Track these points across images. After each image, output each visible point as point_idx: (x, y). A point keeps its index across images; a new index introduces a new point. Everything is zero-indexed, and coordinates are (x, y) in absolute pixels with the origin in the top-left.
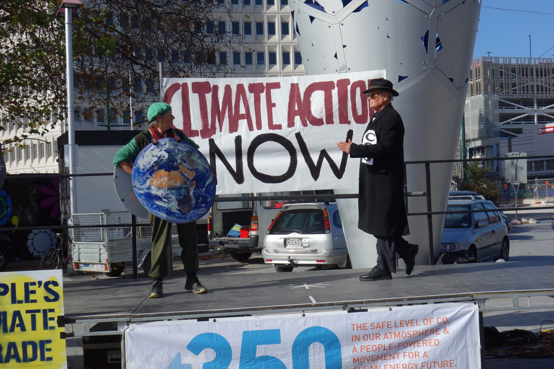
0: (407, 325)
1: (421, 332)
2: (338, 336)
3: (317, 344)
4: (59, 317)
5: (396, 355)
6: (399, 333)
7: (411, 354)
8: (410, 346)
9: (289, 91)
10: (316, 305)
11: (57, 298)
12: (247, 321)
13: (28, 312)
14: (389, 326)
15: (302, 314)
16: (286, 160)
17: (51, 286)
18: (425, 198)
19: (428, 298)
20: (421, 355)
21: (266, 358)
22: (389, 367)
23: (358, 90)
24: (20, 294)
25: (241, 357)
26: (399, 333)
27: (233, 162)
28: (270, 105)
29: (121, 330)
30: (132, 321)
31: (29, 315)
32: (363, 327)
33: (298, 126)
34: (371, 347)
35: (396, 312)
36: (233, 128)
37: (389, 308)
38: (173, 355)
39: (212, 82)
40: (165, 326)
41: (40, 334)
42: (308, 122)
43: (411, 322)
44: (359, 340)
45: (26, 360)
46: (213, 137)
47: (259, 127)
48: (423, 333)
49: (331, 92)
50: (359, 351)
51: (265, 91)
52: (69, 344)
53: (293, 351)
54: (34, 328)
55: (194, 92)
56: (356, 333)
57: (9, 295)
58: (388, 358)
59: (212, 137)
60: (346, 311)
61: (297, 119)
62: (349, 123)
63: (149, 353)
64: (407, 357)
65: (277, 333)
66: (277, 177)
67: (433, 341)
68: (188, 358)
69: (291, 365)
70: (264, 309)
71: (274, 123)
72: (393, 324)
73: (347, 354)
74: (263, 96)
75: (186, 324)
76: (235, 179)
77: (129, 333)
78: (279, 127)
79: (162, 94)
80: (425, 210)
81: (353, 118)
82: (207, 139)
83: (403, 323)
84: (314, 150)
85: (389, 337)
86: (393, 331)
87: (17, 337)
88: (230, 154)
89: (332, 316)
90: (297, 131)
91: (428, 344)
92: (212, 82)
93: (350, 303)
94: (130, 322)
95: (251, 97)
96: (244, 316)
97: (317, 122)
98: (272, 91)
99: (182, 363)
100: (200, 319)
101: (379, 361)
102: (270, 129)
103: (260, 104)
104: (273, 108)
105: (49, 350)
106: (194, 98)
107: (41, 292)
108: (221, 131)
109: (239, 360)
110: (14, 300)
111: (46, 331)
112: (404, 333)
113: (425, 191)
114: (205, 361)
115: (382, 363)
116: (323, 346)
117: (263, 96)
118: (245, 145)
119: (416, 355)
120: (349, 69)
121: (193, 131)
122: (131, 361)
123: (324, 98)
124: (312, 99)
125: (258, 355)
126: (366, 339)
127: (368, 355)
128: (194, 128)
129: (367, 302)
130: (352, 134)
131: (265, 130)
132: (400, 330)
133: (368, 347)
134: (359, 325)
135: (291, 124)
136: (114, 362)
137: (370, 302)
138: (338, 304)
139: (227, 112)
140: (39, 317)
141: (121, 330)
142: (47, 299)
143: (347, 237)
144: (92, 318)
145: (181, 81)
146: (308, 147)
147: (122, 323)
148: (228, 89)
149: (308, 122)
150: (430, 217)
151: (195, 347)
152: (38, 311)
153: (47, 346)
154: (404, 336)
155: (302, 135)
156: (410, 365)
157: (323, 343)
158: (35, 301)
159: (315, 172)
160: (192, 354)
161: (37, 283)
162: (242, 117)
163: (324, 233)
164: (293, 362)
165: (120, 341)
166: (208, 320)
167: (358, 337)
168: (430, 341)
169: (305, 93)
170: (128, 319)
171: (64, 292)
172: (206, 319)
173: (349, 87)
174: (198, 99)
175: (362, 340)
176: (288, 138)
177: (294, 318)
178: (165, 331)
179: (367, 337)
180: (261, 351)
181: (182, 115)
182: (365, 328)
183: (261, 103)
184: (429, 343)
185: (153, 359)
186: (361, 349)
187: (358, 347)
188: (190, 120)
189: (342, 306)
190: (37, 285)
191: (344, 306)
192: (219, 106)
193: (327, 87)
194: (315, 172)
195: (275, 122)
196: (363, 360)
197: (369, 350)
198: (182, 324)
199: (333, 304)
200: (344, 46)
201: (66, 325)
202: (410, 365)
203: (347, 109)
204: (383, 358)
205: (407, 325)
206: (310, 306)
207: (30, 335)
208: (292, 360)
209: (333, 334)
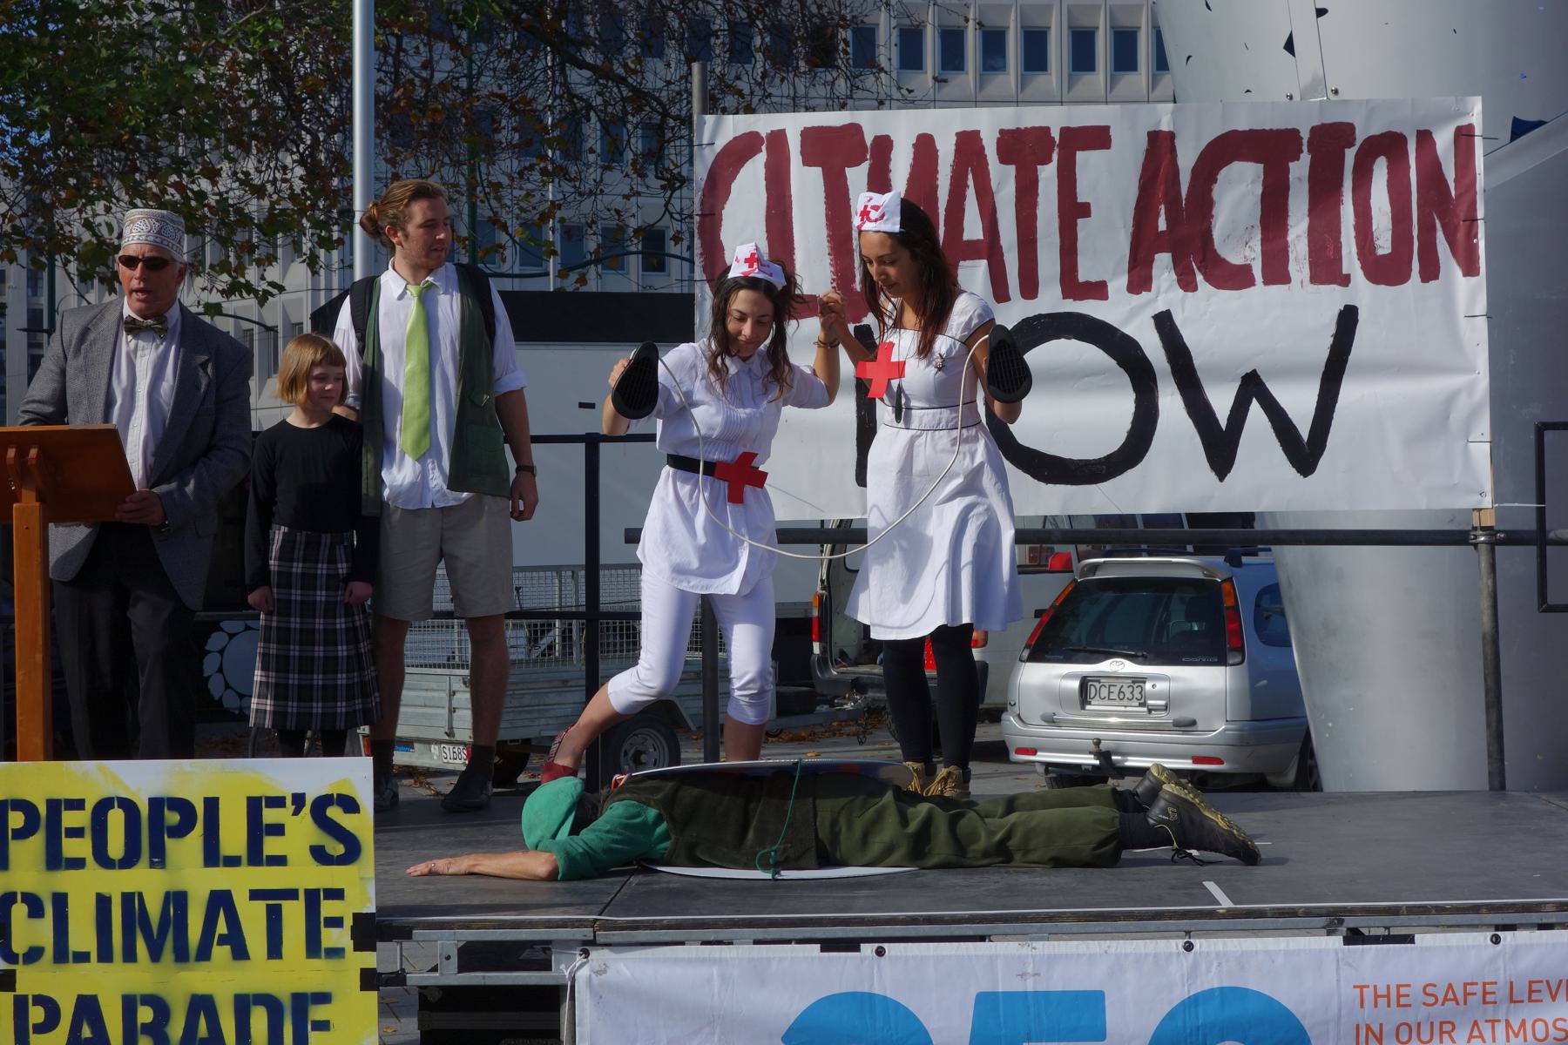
0: (1554, 998)
2: (1306, 1024)
4: (356, 916)
6: (1523, 1023)
10: (1232, 914)
12: (992, 959)
13: (255, 895)
14: (1489, 998)
15: (1181, 942)
17: (334, 813)
24: (233, 838)
26: (1523, 1023)
28: (1073, 210)
29: (563, 968)
30: (600, 940)
31: (261, 906)
32: (1397, 996)
33: (1163, 288)
35: (1516, 950)
37: (1489, 934)
39: (872, 123)
40: (713, 961)
41: (293, 973)
42: (1200, 278)
47: (1030, 289)
52: (387, 1010)
54: (275, 950)
55: (807, 162)
56: (1369, 1015)
57: (196, 836)
61: (1163, 262)
62: (1345, 281)
65: (1093, 1001)
66: (1086, 463)
70: (1050, 918)
71: (1082, 277)
72: (1502, 992)
75: (781, 959)
77: (590, 981)
79: (701, 172)
81: (1358, 264)
84: (1221, 376)
85: (1488, 1035)
89: (1288, 953)
90: (1160, 307)
92: (872, 123)
94: (593, 943)
95: (1003, 179)
96: (982, 938)
97: (1237, 278)
100: (829, 945)
102: (1065, 296)
103: (1034, 205)
104: (1080, 221)
105: (323, 1026)
106: (806, 184)
107: (300, 833)
110: (212, 856)
111: (315, 962)
112: (1540, 1026)
120: (1336, 92)
123: (1259, 189)
126: (1404, 1038)
129: (1412, 911)
131: (1050, 300)
132: (1528, 1012)
134: (1382, 991)
135: (1140, 281)
137: (1424, 910)
138: (1308, 913)
140: (294, 914)
141: (563, 968)
142: (319, 855)
143: (1308, 680)
144: (467, 925)
145: (764, 123)
146: (1198, 361)
147: (567, 945)
148: (925, 147)
149: (1200, 278)
152: (291, 894)
153: (317, 1013)
154: (1541, 1033)
155: (1178, 320)
158: (280, 861)
159: (1221, 448)
161: (289, 801)
162: (972, 251)
163: (1222, 662)
165: (556, 1008)
166: (858, 949)
167: (1377, 1032)
169: (1195, 171)
170: (587, 933)
172: (852, 945)
173: (1350, 155)
176: (1128, 330)
177: (1156, 956)
182: (1403, 1001)
183: (1040, 200)
189: (1323, 921)
190: (290, 807)
191: (1332, 921)
193: (1269, 148)
194: (1221, 448)
195: (1085, 274)
198: (769, 960)
199: (1293, 913)
200: (1321, 12)
201: (379, 944)
203: (1339, 232)
205: (1554, 998)
206: (1211, 915)
207: (260, 974)
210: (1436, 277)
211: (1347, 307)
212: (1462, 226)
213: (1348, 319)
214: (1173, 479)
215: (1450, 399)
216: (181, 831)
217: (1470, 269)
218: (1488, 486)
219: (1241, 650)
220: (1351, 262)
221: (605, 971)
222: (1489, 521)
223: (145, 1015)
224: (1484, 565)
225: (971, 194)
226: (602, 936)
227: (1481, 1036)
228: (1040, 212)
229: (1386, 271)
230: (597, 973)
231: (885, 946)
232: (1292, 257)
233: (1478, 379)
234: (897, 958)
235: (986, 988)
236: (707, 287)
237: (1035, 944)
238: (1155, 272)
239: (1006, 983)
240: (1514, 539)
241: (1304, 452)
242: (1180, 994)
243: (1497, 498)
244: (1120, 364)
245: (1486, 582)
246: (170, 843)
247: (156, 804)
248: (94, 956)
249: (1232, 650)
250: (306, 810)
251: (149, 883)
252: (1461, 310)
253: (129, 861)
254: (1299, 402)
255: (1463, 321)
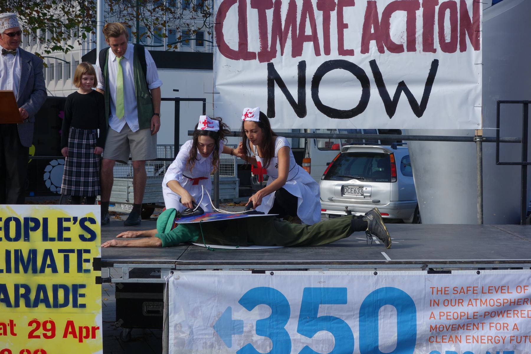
0: (497, 292)
1: (513, 301)
2: (414, 299)
3: (389, 307)
4: (94, 259)
5: (480, 325)
6: (486, 300)
7: (498, 326)
8: (499, 316)
9: (365, 9)
10: (390, 263)
11: (93, 237)
13: (60, 251)
15: (373, 272)
16: (357, 92)
17: (87, 224)
18: (520, 145)
19: (525, 262)
20: (511, 327)
21: (328, 319)
22: (471, 338)
23: (448, 12)
24: (53, 231)
25: (301, 316)
26: (486, 300)
27: (294, 92)
28: (342, 26)
30: (177, 268)
32: (444, 291)
33: (373, 52)
34: (452, 314)
35: (485, 276)
36: (297, 51)
38: (223, 309)
40: (215, 276)
41: (73, 277)
42: (385, 49)
43: (501, 289)
44: (438, 305)
45: (56, 305)
46: (273, 61)
47: (327, 52)
48: (514, 302)
49: (415, 13)
50: (437, 317)
51: (336, 8)
52: (105, 292)
53: (360, 313)
54: (67, 270)
56: (435, 297)
58: (471, 328)
59: (271, 61)
60: (425, 272)
61: (373, 44)
62: (434, 51)
63: (195, 305)
64: (493, 329)
65: (343, 291)
67: (526, 312)
68: (240, 314)
69: (358, 328)
70: (329, 263)
71: (345, 48)
72: (479, 289)
73: (423, 321)
74: (334, 15)
76: (296, 111)
77: (173, 282)
78: (351, 53)
80: (520, 160)
81: (439, 45)
82: (265, 64)
83: (491, 289)
84: (391, 82)
85: (474, 304)
86: (479, 298)
87: (48, 279)
88: (291, 83)
90: (372, 59)
91: (519, 315)
93: (431, 263)
94: (175, 269)
96: (306, 270)
97: (396, 49)
98: (345, 8)
99: (233, 319)
100: (254, 272)
101: (461, 331)
102: (340, 54)
103: (329, 24)
105: (83, 295)
106: (252, 14)
107: (76, 230)
108: (282, 54)
109: (298, 319)
110: (45, 237)
111: (80, 274)
112: (492, 302)
113: (520, 136)
114: (258, 318)
115: (463, 333)
116: (395, 309)
117: (334, 15)
118: (310, 72)
119: (505, 326)
121: (250, 52)
122: (175, 313)
123: (406, 19)
124: (391, 20)
125: (319, 315)
126: (446, 304)
127: (448, 323)
128: (250, 49)
129: (451, 263)
130: (438, 65)
131: (335, 55)
132: (488, 297)
133: (449, 314)
134: (439, 289)
135: (365, 49)
136: (150, 315)
137: (455, 263)
138: (416, 263)
139: (290, 32)
140: (73, 258)
142: (82, 238)
143: (418, 187)
144: (132, 263)
146: (384, 78)
147: (166, 269)
149: (385, 49)
150: (524, 166)
151: (249, 301)
152: (72, 251)
153: (81, 291)
154: (492, 304)
155: (378, 63)
156: (497, 338)
157: (396, 306)
158: (69, 240)
159: (391, 107)
160: (244, 309)
161: (72, 219)
163: (389, 181)
164: (360, 326)
165: (162, 291)
166: (264, 273)
167: (437, 302)
168: (523, 312)
169: (384, 13)
170: (173, 266)
171: (102, 231)
172: (263, 272)
173: (437, 8)
174: (258, 16)
175: (441, 305)
176: (361, 66)
177: (365, 276)
178: (214, 282)
179: (447, 302)
180: (323, 310)
181: (238, 34)
182: (446, 292)
183: (331, 22)
184: (521, 314)
185: (200, 313)
186: (440, 316)
187: (436, 313)
188: (247, 40)
189: (421, 266)
190: (72, 222)
191: (424, 265)
192: (281, 25)
194: (391, 107)
195: (347, 46)
196: (441, 329)
197: (449, 317)
199: (411, 263)
201: (102, 268)
202: (497, 338)
204: (465, 327)
205: (497, 292)
206: (384, 263)
207: (61, 278)
208: (358, 323)
209: (409, 296)
210: (465, 51)
211: (435, 60)
212: (475, 33)
213: (435, 64)
214: (374, 118)
215: (469, 92)
216: (35, 229)
217: (477, 48)
218: (480, 122)
219: (396, 177)
220: (437, 45)
221: (179, 279)
222: (480, 134)
223: (22, 291)
224: (478, 149)
225: (308, 20)
226: (178, 267)
227: (472, 304)
228: (331, 26)
229: (448, 48)
230: (177, 279)
231: (274, 272)
232: (417, 42)
233: (477, 86)
234: (277, 276)
235: (307, 286)
236: (217, 48)
237: (324, 272)
238: (370, 47)
239: (314, 285)
240: (488, 140)
241: (419, 109)
242: (372, 289)
243: (483, 126)
244: (357, 78)
245: (479, 154)
246: (31, 233)
247: (26, 220)
248: (5, 271)
249: (393, 177)
250: (78, 222)
251: (24, 246)
252: (473, 62)
253: (17, 239)
254: (418, 92)
255: (474, 66)
